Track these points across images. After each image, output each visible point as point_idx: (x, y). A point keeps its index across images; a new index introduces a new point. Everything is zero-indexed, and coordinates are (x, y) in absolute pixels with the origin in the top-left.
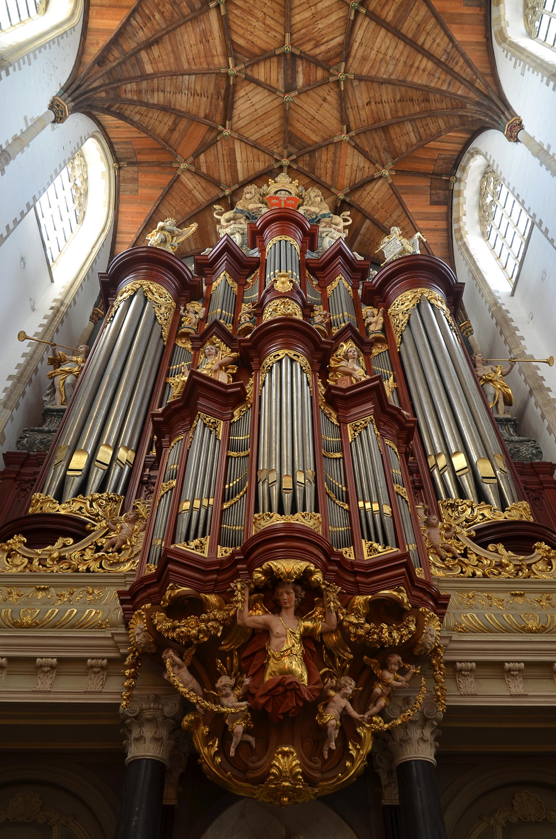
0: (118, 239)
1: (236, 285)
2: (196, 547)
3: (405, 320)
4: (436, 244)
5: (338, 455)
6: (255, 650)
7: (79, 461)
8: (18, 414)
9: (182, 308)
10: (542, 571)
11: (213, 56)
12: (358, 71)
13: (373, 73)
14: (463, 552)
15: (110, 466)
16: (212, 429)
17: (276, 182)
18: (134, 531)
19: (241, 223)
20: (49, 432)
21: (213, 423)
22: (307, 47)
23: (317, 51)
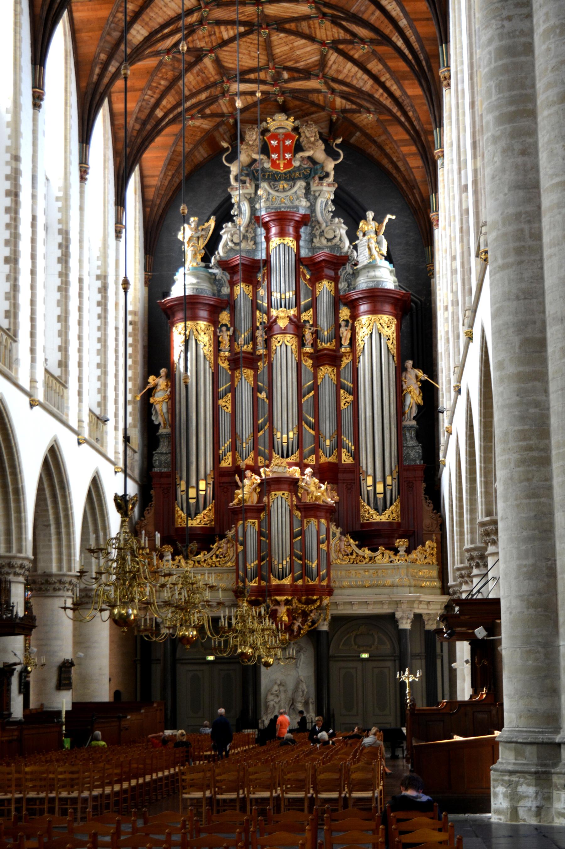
0: (145, 183)
1: (251, 287)
3: (362, 346)
4: (418, 167)
7: (192, 493)
8: (139, 425)
9: (218, 330)
11: (208, 78)
12: (335, 76)
13: (348, 80)
15: (206, 490)
17: (274, 120)
18: (228, 548)
19: (247, 188)
20: (166, 453)
22: (289, 64)
23: (298, 65)
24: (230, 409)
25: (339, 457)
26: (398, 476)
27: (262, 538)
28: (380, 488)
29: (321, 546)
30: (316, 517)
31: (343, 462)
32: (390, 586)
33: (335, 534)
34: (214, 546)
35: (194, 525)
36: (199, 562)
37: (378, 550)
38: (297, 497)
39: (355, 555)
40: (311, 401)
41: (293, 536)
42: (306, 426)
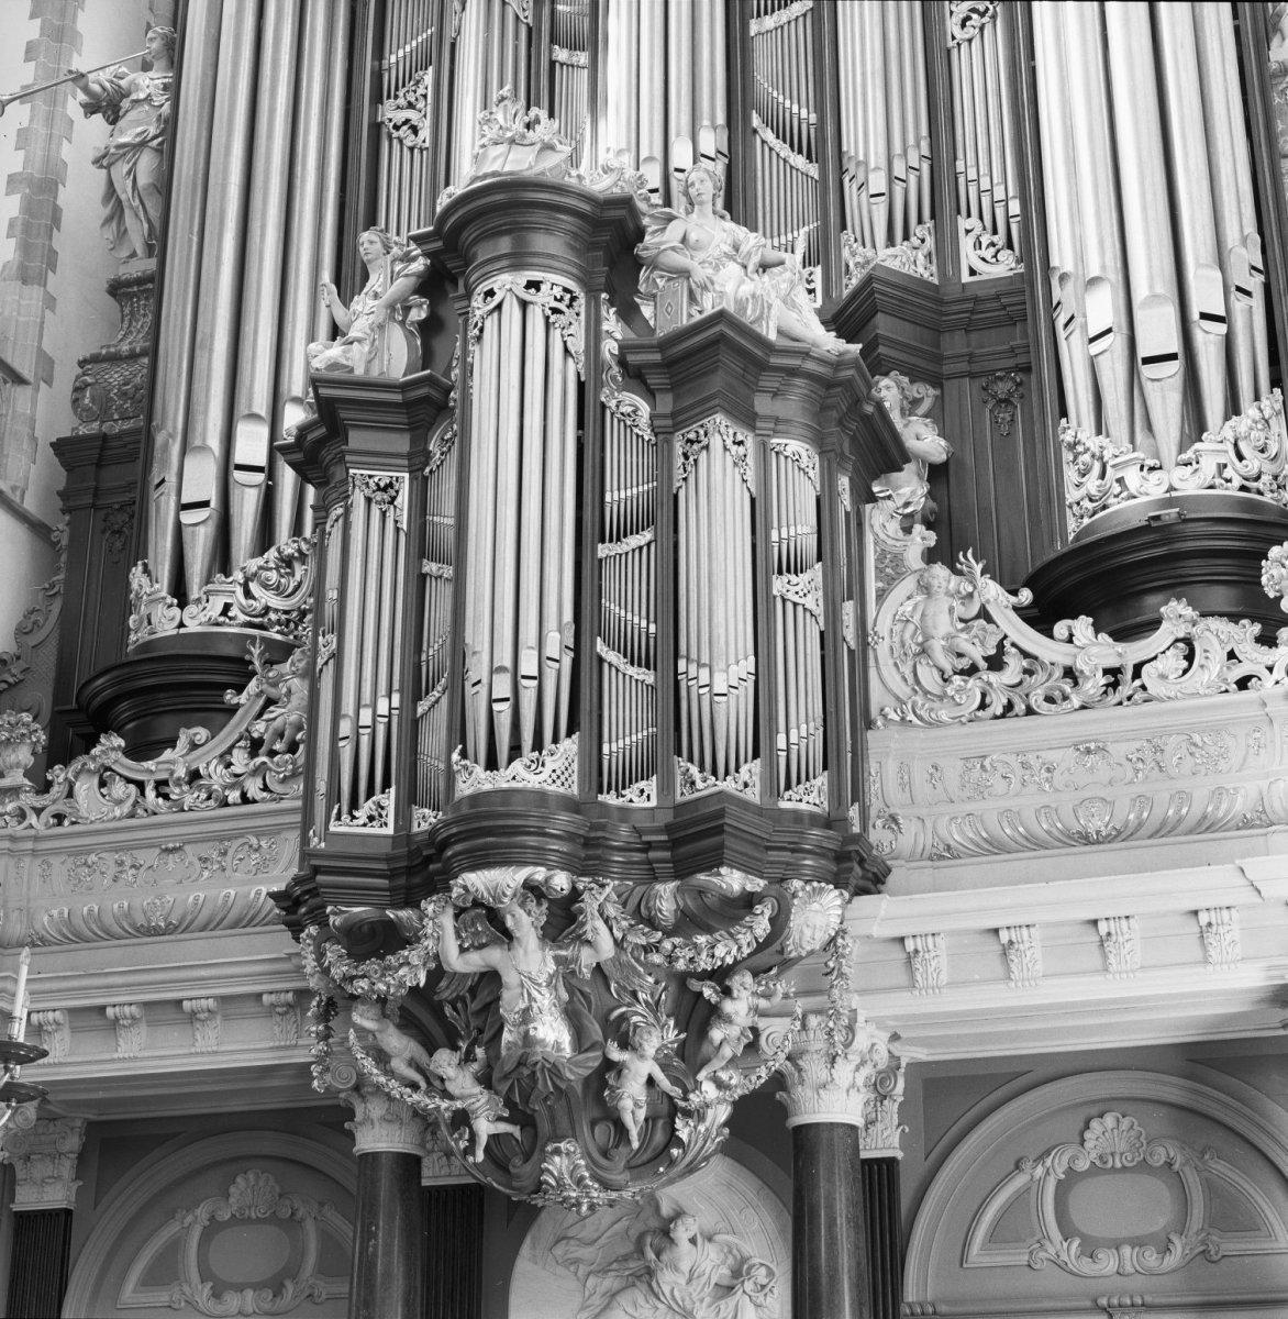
2: (371, 818)
5: (647, 536)
6: (488, 1000)
10: (1163, 677)
14: (992, 652)
16: (384, 507)
21: (384, 489)
24: (425, 133)
25: (945, 251)
26: (1267, 287)
27: (430, 567)
28: (1158, 332)
29: (779, 585)
30: (748, 418)
31: (966, 278)
32: (1247, 824)
33: (898, 560)
34: (243, 698)
35: (193, 627)
36: (161, 785)
37: (1155, 624)
38: (628, 313)
39: (1015, 664)
40: (802, 36)
41: (591, 525)
42: (769, 136)
